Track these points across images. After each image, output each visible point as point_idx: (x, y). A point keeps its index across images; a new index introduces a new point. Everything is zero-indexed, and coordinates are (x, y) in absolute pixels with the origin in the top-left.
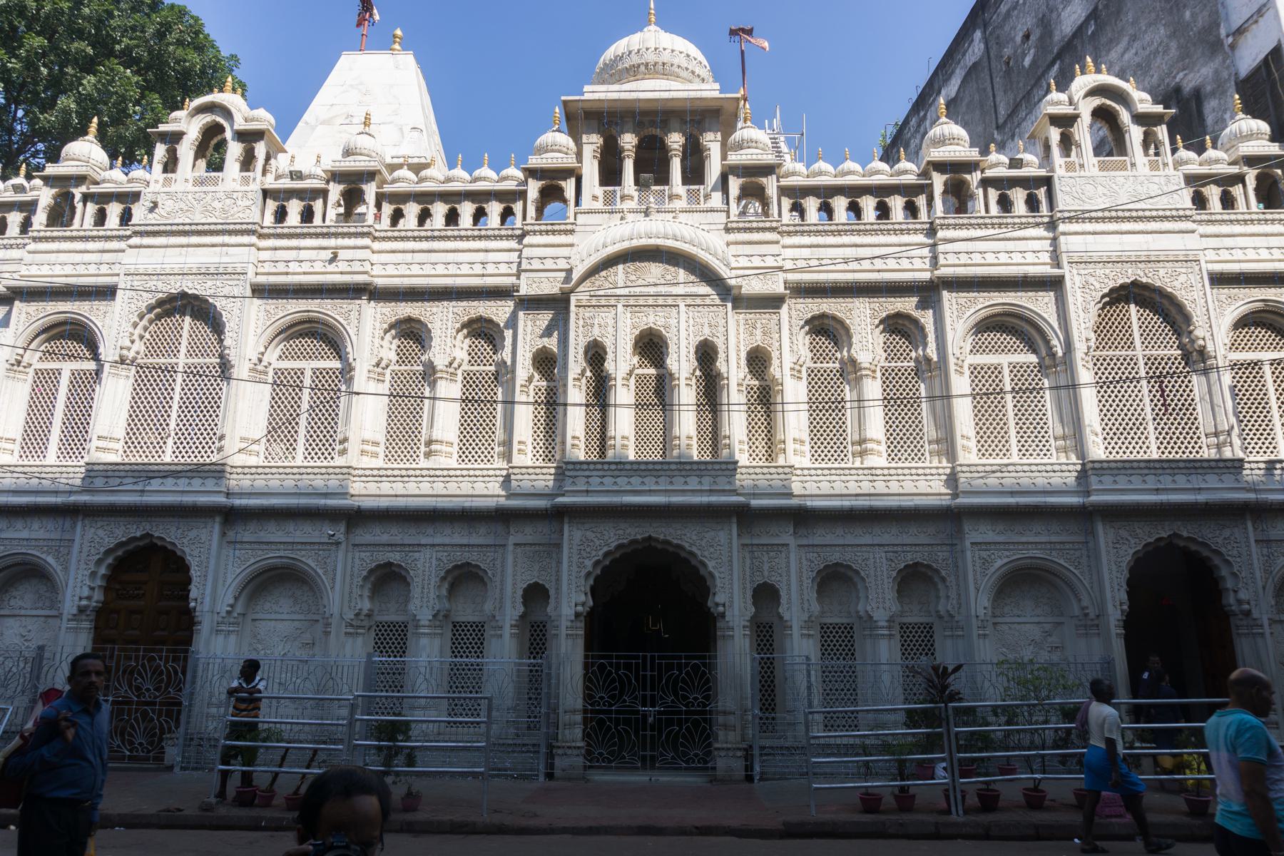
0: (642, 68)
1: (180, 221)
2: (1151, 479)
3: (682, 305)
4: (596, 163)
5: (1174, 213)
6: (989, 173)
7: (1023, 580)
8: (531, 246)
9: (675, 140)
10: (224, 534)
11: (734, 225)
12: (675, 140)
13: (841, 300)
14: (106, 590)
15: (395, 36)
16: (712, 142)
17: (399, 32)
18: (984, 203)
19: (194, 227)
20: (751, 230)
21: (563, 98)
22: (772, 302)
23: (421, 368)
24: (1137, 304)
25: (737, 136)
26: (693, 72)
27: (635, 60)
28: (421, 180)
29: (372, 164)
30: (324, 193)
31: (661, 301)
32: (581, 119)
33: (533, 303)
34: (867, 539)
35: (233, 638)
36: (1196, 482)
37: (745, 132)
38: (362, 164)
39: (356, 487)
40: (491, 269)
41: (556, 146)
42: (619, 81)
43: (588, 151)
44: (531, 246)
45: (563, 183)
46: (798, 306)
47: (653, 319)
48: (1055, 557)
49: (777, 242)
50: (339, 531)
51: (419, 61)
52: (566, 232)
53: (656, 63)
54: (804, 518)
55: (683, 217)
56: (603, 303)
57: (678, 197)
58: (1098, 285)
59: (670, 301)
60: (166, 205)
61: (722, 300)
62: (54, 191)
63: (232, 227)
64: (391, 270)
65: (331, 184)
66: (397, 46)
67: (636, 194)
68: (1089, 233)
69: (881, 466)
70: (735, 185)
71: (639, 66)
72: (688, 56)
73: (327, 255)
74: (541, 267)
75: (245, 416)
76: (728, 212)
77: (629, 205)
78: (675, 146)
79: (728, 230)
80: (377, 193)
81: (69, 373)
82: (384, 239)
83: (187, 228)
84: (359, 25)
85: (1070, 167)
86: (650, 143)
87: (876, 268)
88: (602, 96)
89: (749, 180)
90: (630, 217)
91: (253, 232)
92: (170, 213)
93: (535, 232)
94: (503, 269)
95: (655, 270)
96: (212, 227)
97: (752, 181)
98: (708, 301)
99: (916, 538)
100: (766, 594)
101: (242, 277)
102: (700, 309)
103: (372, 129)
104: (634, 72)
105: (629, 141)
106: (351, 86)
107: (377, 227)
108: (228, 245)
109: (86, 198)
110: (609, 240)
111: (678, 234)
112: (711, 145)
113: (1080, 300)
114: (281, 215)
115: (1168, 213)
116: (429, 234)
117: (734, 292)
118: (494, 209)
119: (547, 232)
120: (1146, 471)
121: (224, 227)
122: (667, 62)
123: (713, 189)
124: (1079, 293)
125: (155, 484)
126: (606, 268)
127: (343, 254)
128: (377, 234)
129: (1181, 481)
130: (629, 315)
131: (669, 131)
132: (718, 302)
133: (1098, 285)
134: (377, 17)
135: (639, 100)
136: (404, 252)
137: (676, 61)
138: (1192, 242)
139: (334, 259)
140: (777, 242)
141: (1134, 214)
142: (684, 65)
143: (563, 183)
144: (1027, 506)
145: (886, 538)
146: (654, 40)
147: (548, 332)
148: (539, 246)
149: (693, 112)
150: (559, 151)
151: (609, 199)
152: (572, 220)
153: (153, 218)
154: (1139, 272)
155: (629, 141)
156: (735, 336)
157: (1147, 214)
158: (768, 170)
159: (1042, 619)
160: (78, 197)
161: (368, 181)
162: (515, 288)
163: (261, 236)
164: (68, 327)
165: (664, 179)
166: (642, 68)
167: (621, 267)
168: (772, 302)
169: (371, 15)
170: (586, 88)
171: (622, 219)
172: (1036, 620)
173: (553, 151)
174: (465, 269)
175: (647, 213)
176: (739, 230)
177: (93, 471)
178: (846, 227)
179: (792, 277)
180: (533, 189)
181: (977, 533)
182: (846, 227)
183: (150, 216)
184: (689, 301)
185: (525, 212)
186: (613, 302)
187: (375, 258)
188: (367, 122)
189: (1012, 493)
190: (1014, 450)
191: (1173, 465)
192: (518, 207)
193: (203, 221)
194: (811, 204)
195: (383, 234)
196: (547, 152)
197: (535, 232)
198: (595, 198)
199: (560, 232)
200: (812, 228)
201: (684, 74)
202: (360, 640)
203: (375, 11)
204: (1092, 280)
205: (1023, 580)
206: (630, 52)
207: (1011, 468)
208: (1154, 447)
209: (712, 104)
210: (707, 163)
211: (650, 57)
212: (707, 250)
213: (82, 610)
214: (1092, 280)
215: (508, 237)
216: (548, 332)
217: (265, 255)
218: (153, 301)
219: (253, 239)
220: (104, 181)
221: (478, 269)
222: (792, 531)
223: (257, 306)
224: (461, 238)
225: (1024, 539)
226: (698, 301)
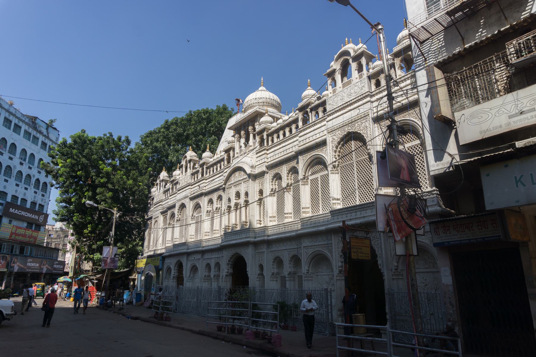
2: (354, 214)
5: (362, 97)
6: (313, 105)
7: (319, 260)
10: (187, 258)
14: (178, 272)
18: (312, 118)
22: (262, 174)
24: (354, 140)
34: (283, 248)
35: (191, 283)
36: (364, 214)
39: (204, 244)
47: (238, 189)
48: (320, 249)
50: (199, 256)
54: (269, 243)
58: (336, 138)
68: (335, 118)
69: (291, 221)
75: (192, 230)
85: (344, 86)
91: (189, 185)
95: (237, 174)
99: (293, 245)
100: (261, 267)
113: (331, 146)
115: (360, 98)
120: (347, 212)
124: (331, 144)
125: (180, 248)
129: (359, 214)
133: (336, 138)
138: (363, 109)
141: (348, 103)
144: (313, 232)
145: (288, 247)
154: (350, 128)
156: (253, 187)
157: (353, 101)
159: (328, 273)
163: (192, 185)
168: (262, 174)
172: (327, 274)
177: (175, 246)
181: (306, 243)
189: (313, 227)
190: (321, 209)
191: (352, 209)
202: (207, 283)
204: (334, 137)
205: (319, 260)
207: (313, 218)
208: (358, 201)
213: (174, 277)
214: (334, 137)
217: (192, 190)
219: (190, 187)
222: (265, 247)
225: (316, 244)
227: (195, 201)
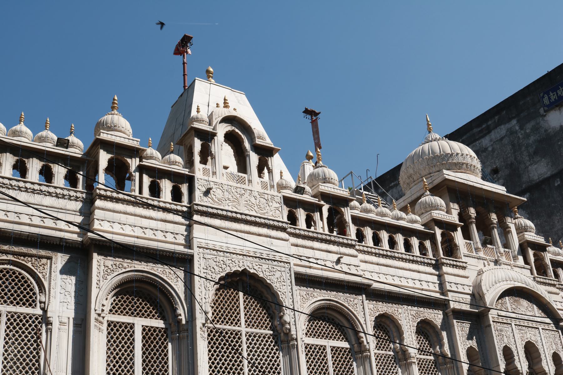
0: (465, 166)
1: (230, 209)
9: (494, 217)
19: (244, 217)
23: (391, 353)
27: (461, 160)
30: (319, 208)
33: (460, 315)
56: (505, 321)
60: (217, 193)
62: (109, 156)
63: (271, 223)
65: (322, 203)
71: (463, 164)
73: (336, 257)
77: (481, 254)
81: (141, 329)
83: (239, 216)
92: (220, 200)
94: (432, 287)
95: (525, 303)
96: (258, 220)
101: (286, 265)
102: (547, 332)
108: (270, 237)
109: (142, 169)
114: (292, 219)
116: (411, 258)
121: (267, 221)
127: (345, 260)
130: (518, 331)
131: (489, 212)
132: (555, 329)
135: (482, 189)
136: (372, 263)
139: (338, 261)
147: (470, 338)
153: (206, 201)
155: (472, 211)
160: (133, 168)
164: (134, 285)
166: (465, 166)
167: (507, 298)
170: (445, 172)
175: (496, 262)
183: (205, 199)
187: (363, 266)
193: (247, 212)
216: (470, 338)
218: (223, 274)
220: (151, 158)
223: (300, 292)
227: (320, 296)
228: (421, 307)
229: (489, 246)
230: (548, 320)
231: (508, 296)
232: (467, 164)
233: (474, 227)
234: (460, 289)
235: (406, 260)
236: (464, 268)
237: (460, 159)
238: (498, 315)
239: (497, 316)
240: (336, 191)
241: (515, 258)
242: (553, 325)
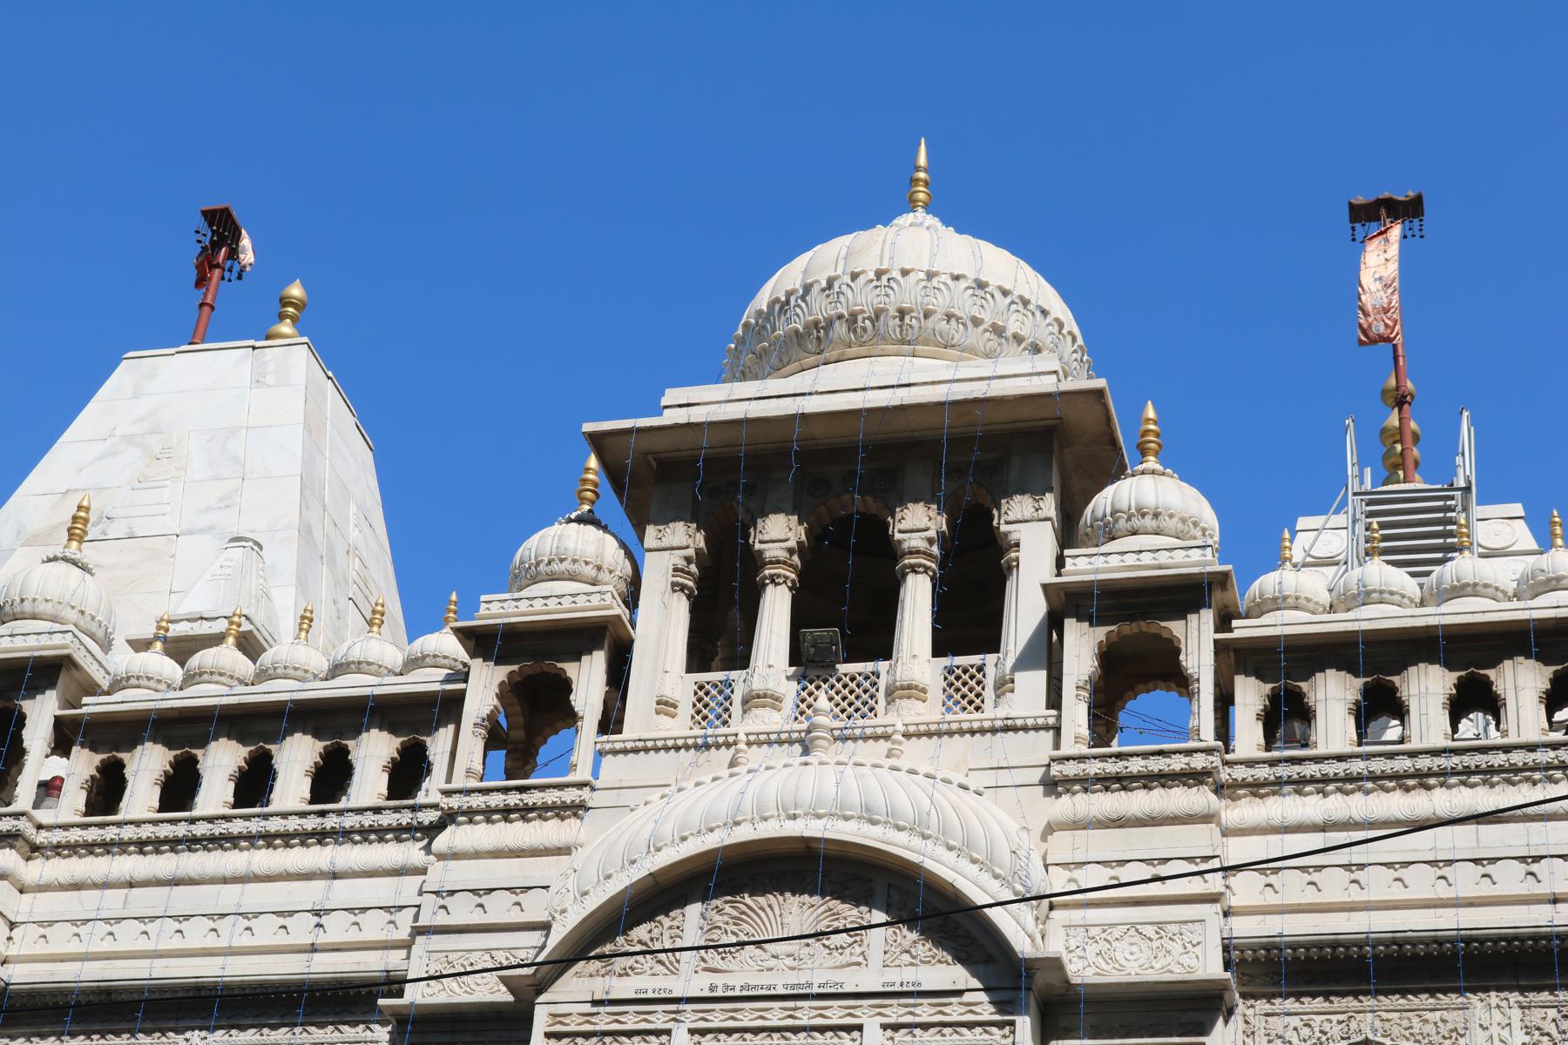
0: (840, 329)
3: (872, 1025)
4: (680, 609)
8: (456, 856)
9: (918, 525)
11: (1071, 769)
12: (918, 525)
13: (1424, 1000)
15: (285, 302)
16: (1030, 527)
17: (296, 291)
20: (1123, 782)
21: (588, 427)
25: (1105, 500)
26: (998, 331)
27: (820, 308)
28: (190, 679)
29: (58, 640)
31: (806, 1014)
32: (654, 478)
37: (1146, 488)
38: (32, 641)
40: (337, 929)
41: (574, 560)
42: (777, 370)
43: (658, 571)
44: (456, 856)
45: (570, 669)
46: (1276, 1024)
49: (1207, 818)
51: (337, 358)
52: (563, 811)
53: (878, 313)
55: (917, 753)
57: (912, 690)
59: (836, 1013)
61: (1002, 1006)
64: (61, 940)
66: (286, 328)
67: (790, 690)
70: (1082, 648)
71: (830, 323)
72: (981, 285)
74: (477, 918)
76: (1057, 730)
78: (916, 541)
79: (1052, 786)
80: (59, 722)
82: (58, 849)
84: (201, 281)
86: (847, 533)
87: (1544, 889)
88: (698, 415)
89: (1129, 628)
90: (755, 756)
93: (470, 814)
95: (797, 912)
97: (1136, 638)
98: (955, 1012)
103: (88, 553)
104: (814, 342)
105: (779, 534)
106: (128, 439)
107: (44, 816)
110: (668, 830)
111: (879, 802)
112: (1019, 533)
117: (1041, 979)
118: (373, 753)
119: (506, 813)
122: (938, 305)
123: (1024, 663)
126: (649, 917)
128: (41, 838)
132: (987, 1012)
134: (248, 256)
135: (804, 417)
137: (939, 302)
140: (1207, 818)
142: (966, 305)
143: (570, 669)
146: (919, 251)
148: (477, 855)
149: (961, 442)
150: (572, 577)
151: (710, 707)
152: (582, 774)
155: (779, 534)
158: (1185, 594)
161: (34, 690)
162: (394, 984)
165: (876, 640)
166: (840, 329)
167: (694, 910)
169: (233, 254)
170: (671, 396)
171: (732, 764)
173: (553, 577)
174: (266, 932)
176: (1087, 783)
178: (1443, 762)
179: (1247, 928)
180: (484, 689)
182: (1443, 762)
184: (896, 1012)
185: (458, 755)
186: (659, 1022)
188: (77, 528)
192: (438, 744)
194: (1333, 697)
195: (58, 836)
196: (535, 580)
197: (470, 814)
198: (666, 706)
199: (543, 811)
200: (1332, 769)
201: (975, 337)
203: (246, 241)
206: (807, 288)
209: (1027, 412)
210: (1010, 586)
211: (863, 298)
212: (963, 849)
215: (401, 833)
221: (302, 930)
224: (269, 839)
226: (925, 1011)
228: (274, 1027)
229: (843, 668)
230: (955, 975)
231: (704, 899)
232: (853, 319)
233: (776, 609)
234: (500, 909)
235: (174, 844)
236: (578, 809)
237: (816, 306)
238: (595, 1003)
239: (588, 1008)
240: (19, 642)
241: (1004, 686)
242: (983, 997)
